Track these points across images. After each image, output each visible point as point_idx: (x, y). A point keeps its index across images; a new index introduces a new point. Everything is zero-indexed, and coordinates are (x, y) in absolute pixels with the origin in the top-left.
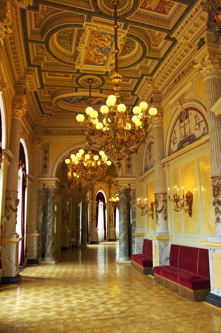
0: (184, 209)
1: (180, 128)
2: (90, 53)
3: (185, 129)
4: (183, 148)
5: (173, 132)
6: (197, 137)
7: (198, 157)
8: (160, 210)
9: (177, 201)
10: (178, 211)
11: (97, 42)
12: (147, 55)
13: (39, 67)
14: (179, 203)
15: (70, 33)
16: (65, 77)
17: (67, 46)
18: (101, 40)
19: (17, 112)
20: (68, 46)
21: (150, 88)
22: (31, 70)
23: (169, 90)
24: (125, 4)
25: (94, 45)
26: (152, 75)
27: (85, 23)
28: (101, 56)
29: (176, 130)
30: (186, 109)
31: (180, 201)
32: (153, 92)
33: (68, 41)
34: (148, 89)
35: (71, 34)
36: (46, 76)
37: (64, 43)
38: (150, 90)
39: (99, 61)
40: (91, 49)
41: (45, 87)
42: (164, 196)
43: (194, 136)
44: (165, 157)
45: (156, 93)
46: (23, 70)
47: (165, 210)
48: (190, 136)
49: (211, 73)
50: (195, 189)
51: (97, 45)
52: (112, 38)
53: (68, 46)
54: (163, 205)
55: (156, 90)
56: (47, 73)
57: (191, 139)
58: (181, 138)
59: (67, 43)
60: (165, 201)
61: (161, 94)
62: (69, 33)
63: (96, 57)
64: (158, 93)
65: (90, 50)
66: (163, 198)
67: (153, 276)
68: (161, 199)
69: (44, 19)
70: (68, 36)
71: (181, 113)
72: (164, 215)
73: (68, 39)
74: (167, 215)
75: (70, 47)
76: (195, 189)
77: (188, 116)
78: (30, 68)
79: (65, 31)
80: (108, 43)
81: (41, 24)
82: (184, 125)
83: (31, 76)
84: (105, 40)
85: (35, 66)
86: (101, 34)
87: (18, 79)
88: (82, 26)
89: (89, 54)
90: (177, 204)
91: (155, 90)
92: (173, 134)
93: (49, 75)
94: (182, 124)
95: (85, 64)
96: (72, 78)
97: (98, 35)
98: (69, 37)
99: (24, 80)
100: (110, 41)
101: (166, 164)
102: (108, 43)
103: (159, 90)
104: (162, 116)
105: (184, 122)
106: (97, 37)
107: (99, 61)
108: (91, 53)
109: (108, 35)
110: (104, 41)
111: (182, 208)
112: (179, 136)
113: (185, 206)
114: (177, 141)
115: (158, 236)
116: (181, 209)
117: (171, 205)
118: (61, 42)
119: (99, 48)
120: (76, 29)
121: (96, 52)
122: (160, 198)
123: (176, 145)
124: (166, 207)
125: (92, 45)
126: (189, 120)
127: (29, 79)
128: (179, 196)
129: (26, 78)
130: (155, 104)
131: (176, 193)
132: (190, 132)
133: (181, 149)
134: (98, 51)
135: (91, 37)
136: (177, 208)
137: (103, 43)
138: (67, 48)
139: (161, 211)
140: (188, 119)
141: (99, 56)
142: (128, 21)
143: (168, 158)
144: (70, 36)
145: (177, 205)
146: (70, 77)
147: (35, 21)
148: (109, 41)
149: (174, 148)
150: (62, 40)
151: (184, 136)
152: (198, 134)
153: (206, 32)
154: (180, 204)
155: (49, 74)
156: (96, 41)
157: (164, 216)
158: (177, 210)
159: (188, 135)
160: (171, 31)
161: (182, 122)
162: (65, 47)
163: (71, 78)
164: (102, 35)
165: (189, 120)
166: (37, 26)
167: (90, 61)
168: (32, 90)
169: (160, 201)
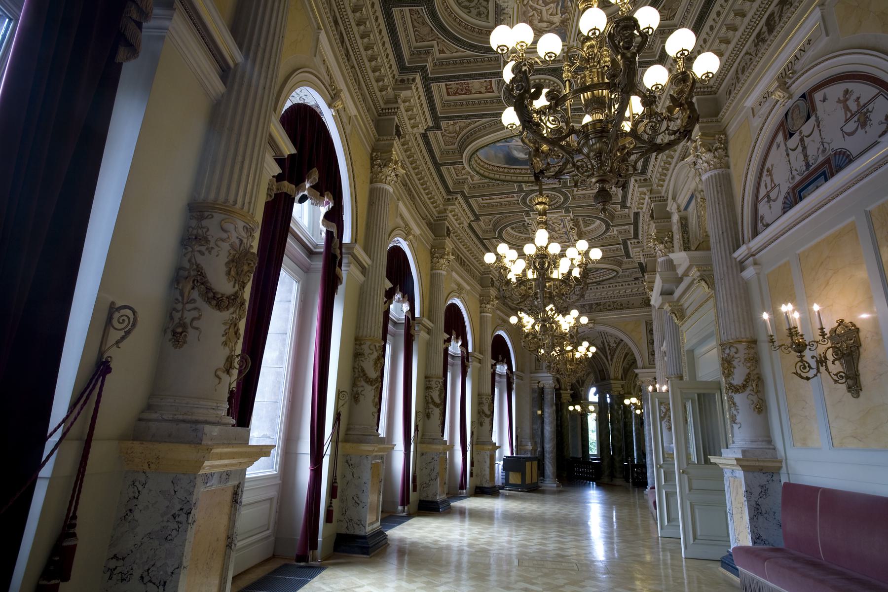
0: (829, 373)
1: (788, 155)
5: (765, 173)
7: (868, 209)
9: (800, 348)
10: (808, 379)
19: (381, 172)
23: (740, 72)
29: (772, 166)
30: (803, 96)
31: (814, 348)
36: (439, 89)
41: (443, 124)
46: (388, 81)
47: (755, 383)
54: (748, 371)
58: (793, 178)
64: (710, 93)
71: (786, 115)
82: (802, 140)
85: (414, 70)
87: (383, 106)
92: (765, 178)
94: (794, 141)
99: (395, 105)
104: (726, 149)
111: (822, 369)
113: (829, 363)
114: (780, 191)
117: (777, 366)
127: (404, 102)
129: (399, 101)
136: (805, 368)
138: (479, 14)
139: (744, 387)
151: (804, 168)
154: (813, 357)
158: (804, 375)
159: (816, 160)
161: (791, 135)
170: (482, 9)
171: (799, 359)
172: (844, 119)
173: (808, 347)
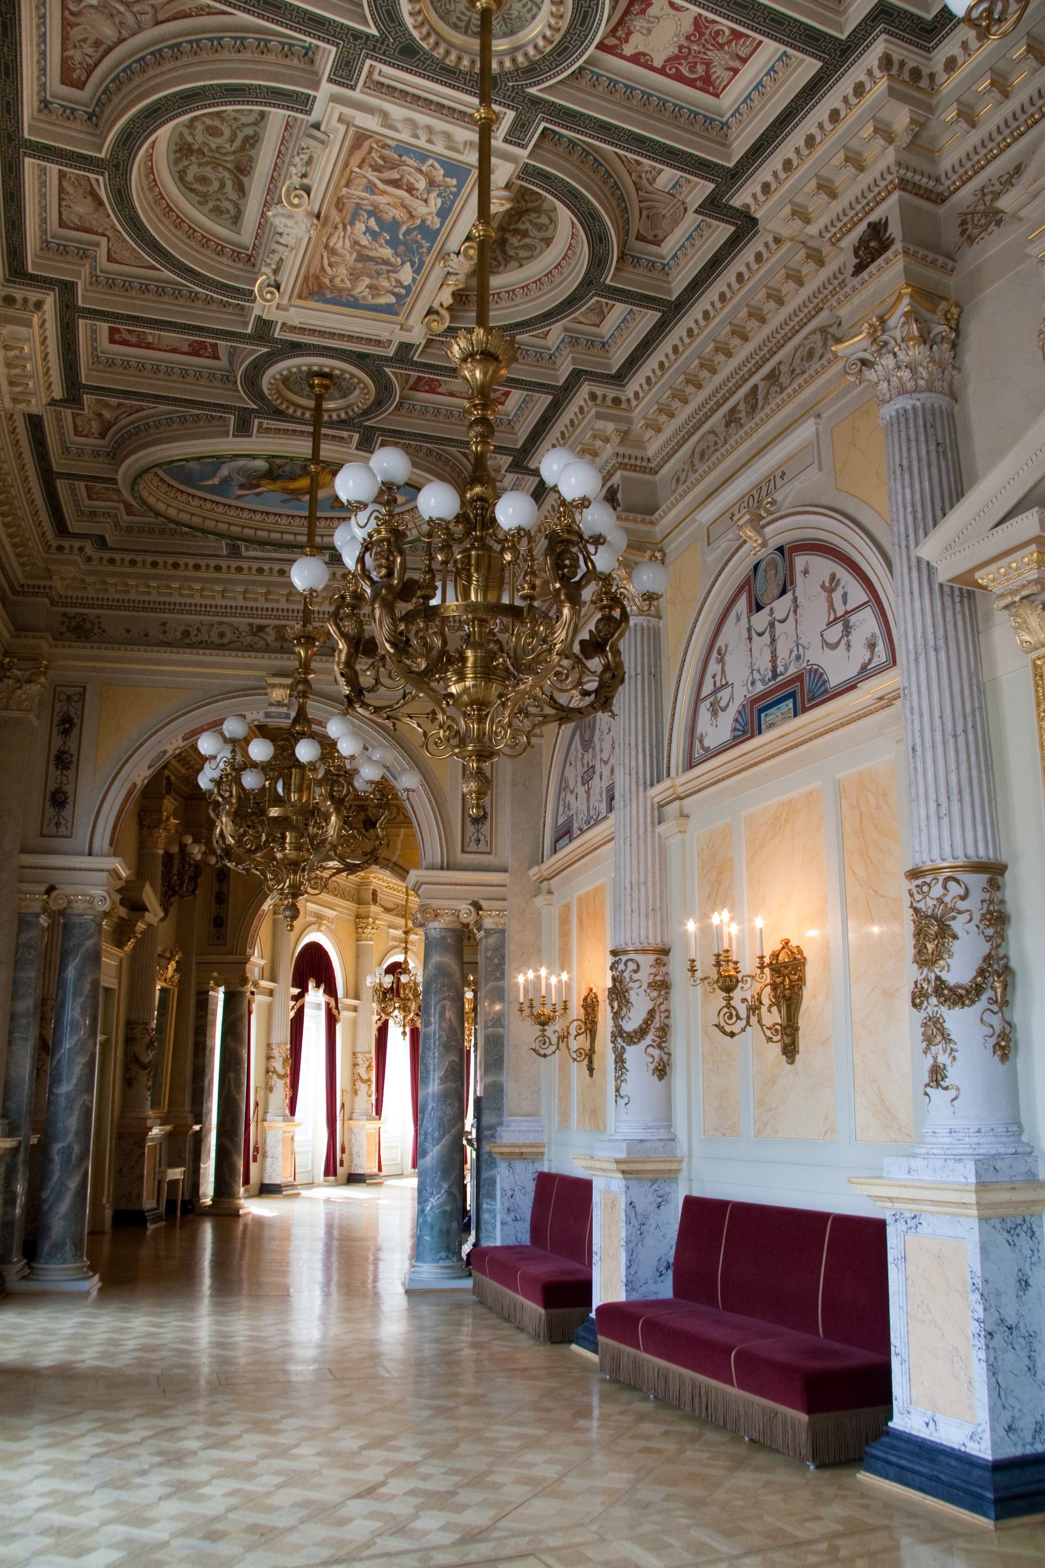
0: (762, 1026)
1: (750, 639)
2: (331, 244)
3: (773, 640)
4: (760, 733)
5: (715, 654)
6: (834, 680)
7: (838, 776)
8: (635, 1031)
9: (728, 985)
10: (732, 1035)
11: (373, 193)
12: (608, 282)
13: (67, 289)
14: (737, 994)
15: (240, 136)
16: (195, 353)
18: (396, 183)
20: (227, 199)
21: (607, 440)
22: (26, 301)
23: (697, 456)
24: (529, 16)
25: (358, 204)
26: (620, 378)
27: (326, 88)
28: (386, 262)
29: (727, 646)
30: (780, 549)
32: (620, 459)
33: (227, 175)
34: (599, 443)
35: (247, 139)
37: (204, 180)
38: (608, 451)
39: (370, 287)
40: (340, 226)
41: (87, 399)
42: (659, 963)
43: (821, 675)
44: (669, 775)
45: (634, 468)
47: (657, 1029)
48: (799, 678)
49: (916, 385)
50: (813, 933)
52: (448, 180)
53: (227, 199)
55: (635, 452)
56: (104, 327)
57: (799, 692)
58: (753, 683)
59: (223, 185)
60: (662, 986)
61: (656, 473)
63: (360, 265)
64: (643, 470)
65: (336, 228)
66: (654, 970)
67: (595, 1351)
68: (645, 976)
69: (117, 44)
70: (228, 146)
71: (756, 567)
72: (656, 1052)
73: (229, 166)
74: (669, 1054)
76: (813, 933)
77: (792, 583)
78: (19, 294)
79: (217, 123)
80: (426, 201)
81: (96, 65)
82: (772, 625)
83: (23, 331)
84: (417, 185)
85: (44, 283)
86: (400, 156)
89: (326, 246)
90: (731, 998)
91: (628, 451)
92: (713, 667)
93: (112, 341)
95: (300, 297)
96: (231, 363)
97: (382, 157)
98: (234, 153)
100: (439, 195)
101: (673, 808)
102: (426, 201)
103: (651, 452)
105: (768, 608)
106: (376, 168)
107: (370, 287)
108: (340, 244)
109: (430, 162)
110: (411, 189)
111: (754, 1019)
112: (743, 674)
113: (764, 1009)
114: (732, 698)
115: (622, 1155)
116: (748, 1023)
117: (693, 1007)
118: (190, 178)
119: (379, 221)
120: (278, 115)
121: (364, 241)
122: (635, 972)
123: (727, 721)
124: (668, 1017)
125: (350, 207)
126: (795, 599)
128: (736, 963)
130: (627, 519)
131: (726, 947)
132: (798, 658)
133: (752, 736)
134: (375, 236)
135: (346, 165)
136: (730, 1017)
137: (402, 200)
138: (218, 211)
140: (789, 596)
141: (377, 263)
142: (535, 101)
143: (681, 780)
144: (243, 148)
145: (729, 1006)
146: (217, 358)
148: (433, 195)
149: (716, 730)
150: (199, 165)
151: (770, 675)
152: (837, 668)
153: (896, 195)
154: (744, 1000)
155: (112, 331)
156: (371, 188)
157: (657, 1059)
158: (728, 1029)
159: (786, 668)
160: (733, 176)
161: (759, 608)
162: (211, 204)
163: (224, 363)
164: (404, 158)
165: (795, 599)
166: (75, 76)
167: (327, 281)
168: (22, 407)
169: (637, 984)
171: (724, 1003)
172: (825, 621)
173: (740, 984)
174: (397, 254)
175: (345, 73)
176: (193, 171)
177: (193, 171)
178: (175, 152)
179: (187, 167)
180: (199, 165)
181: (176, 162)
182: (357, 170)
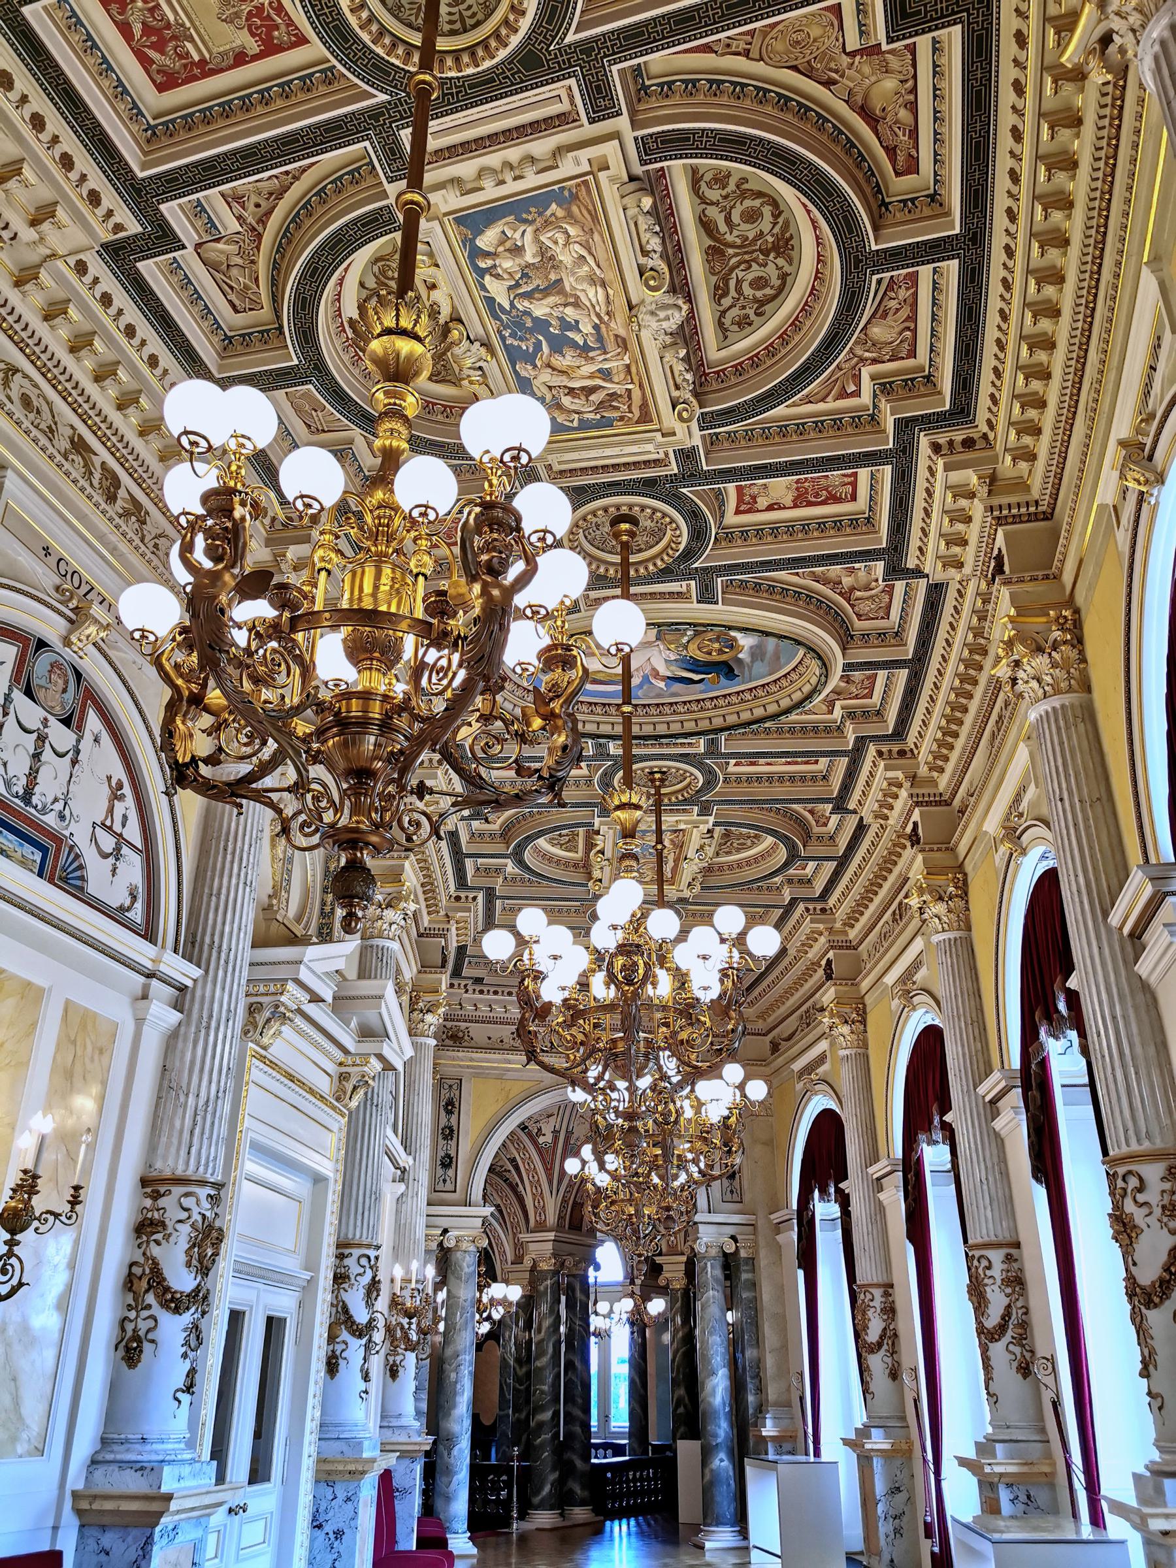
2: (600, 290)
11: (599, 371)
15: (733, 293)
17: (725, 197)
18: (589, 391)
20: (717, 204)
25: (605, 353)
27: (697, 441)
28: (528, 296)
31: (42, 1229)
33: (729, 238)
35: (726, 294)
37: (751, 216)
39: (517, 250)
40: (606, 318)
43: (77, 856)
51: (591, 354)
53: (717, 204)
59: (728, 220)
62: (739, 290)
63: (553, 277)
70: (741, 274)
73: (731, 251)
75: (703, 200)
79: (759, 294)
80: (550, 388)
84: (569, 398)
88: (706, 421)
89: (604, 285)
90: (18, 1243)
98: (732, 269)
102: (550, 388)
106: (613, 396)
107: (517, 250)
108: (591, 294)
109: (575, 424)
110: (571, 391)
118: (767, 211)
119: (574, 345)
121: (570, 313)
125: (611, 345)
134: (566, 325)
135: (641, 386)
141: (537, 289)
144: (726, 280)
147: (915, 295)
150: (761, 234)
156: (606, 375)
162: (732, 187)
167: (572, 231)
170: (714, 195)
174: (527, 313)
175: (687, 456)
176: (765, 225)
177: (765, 225)
178: (791, 237)
179: (775, 224)
180: (761, 234)
181: (787, 224)
182: (630, 386)
